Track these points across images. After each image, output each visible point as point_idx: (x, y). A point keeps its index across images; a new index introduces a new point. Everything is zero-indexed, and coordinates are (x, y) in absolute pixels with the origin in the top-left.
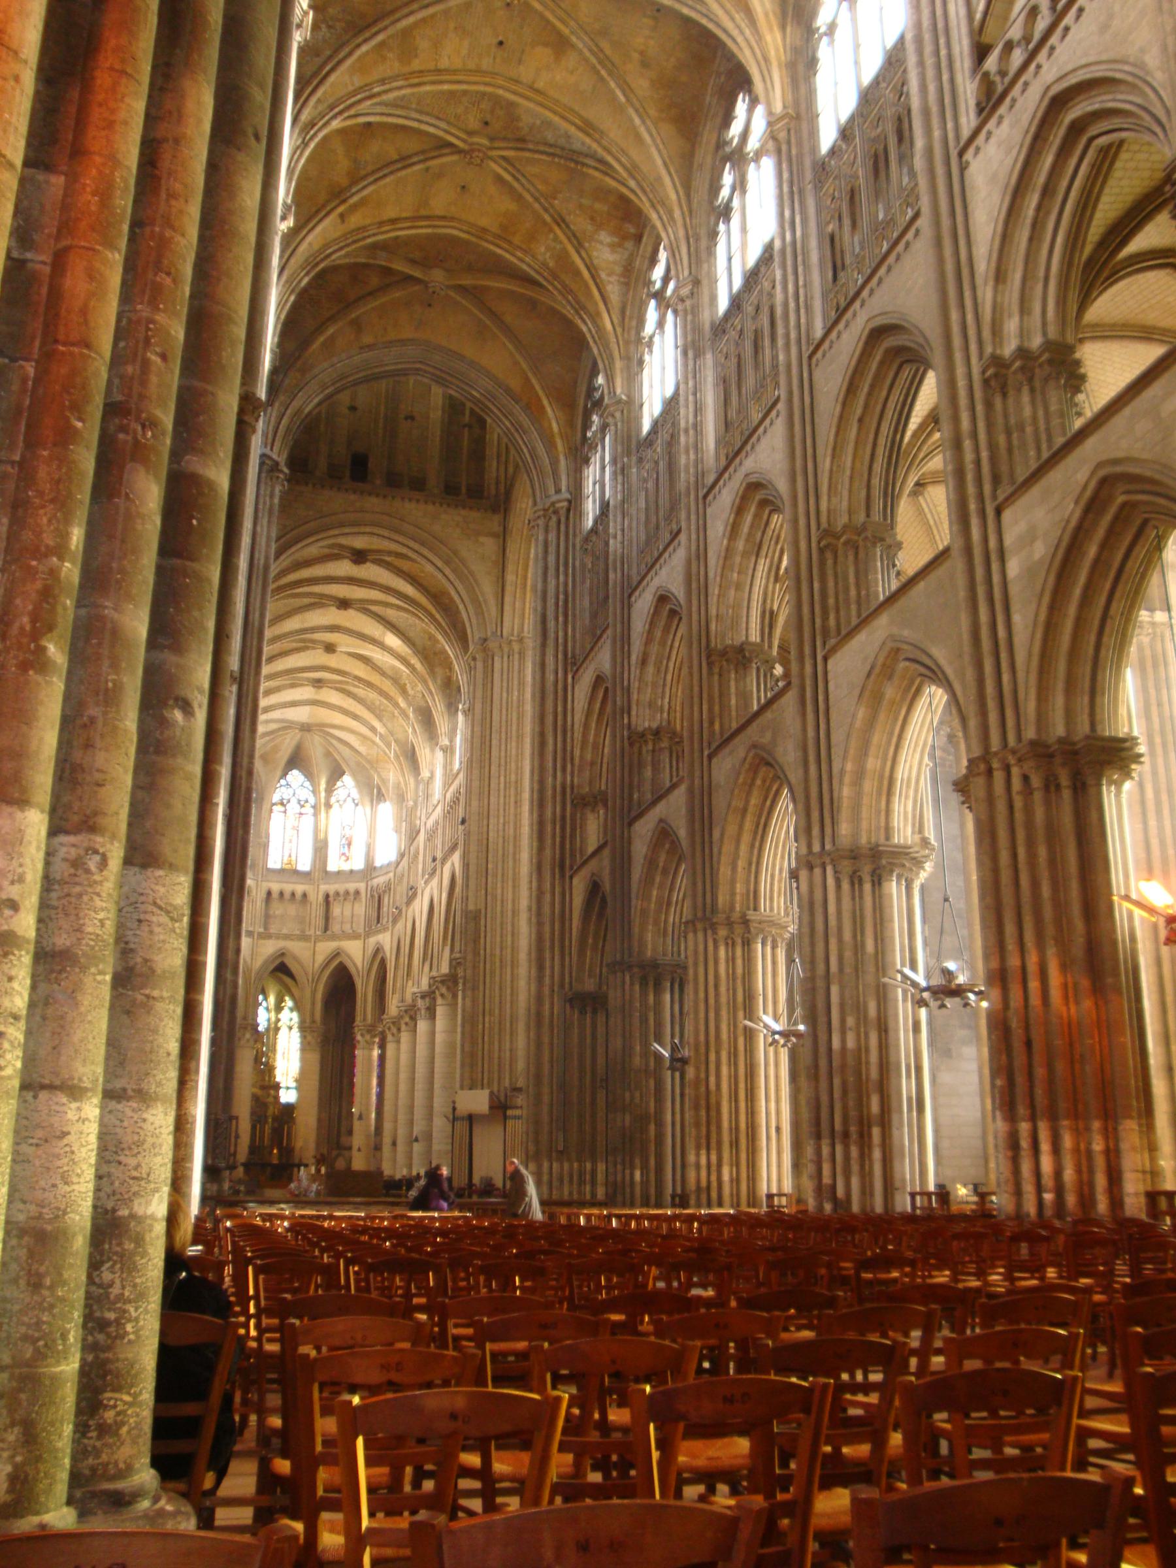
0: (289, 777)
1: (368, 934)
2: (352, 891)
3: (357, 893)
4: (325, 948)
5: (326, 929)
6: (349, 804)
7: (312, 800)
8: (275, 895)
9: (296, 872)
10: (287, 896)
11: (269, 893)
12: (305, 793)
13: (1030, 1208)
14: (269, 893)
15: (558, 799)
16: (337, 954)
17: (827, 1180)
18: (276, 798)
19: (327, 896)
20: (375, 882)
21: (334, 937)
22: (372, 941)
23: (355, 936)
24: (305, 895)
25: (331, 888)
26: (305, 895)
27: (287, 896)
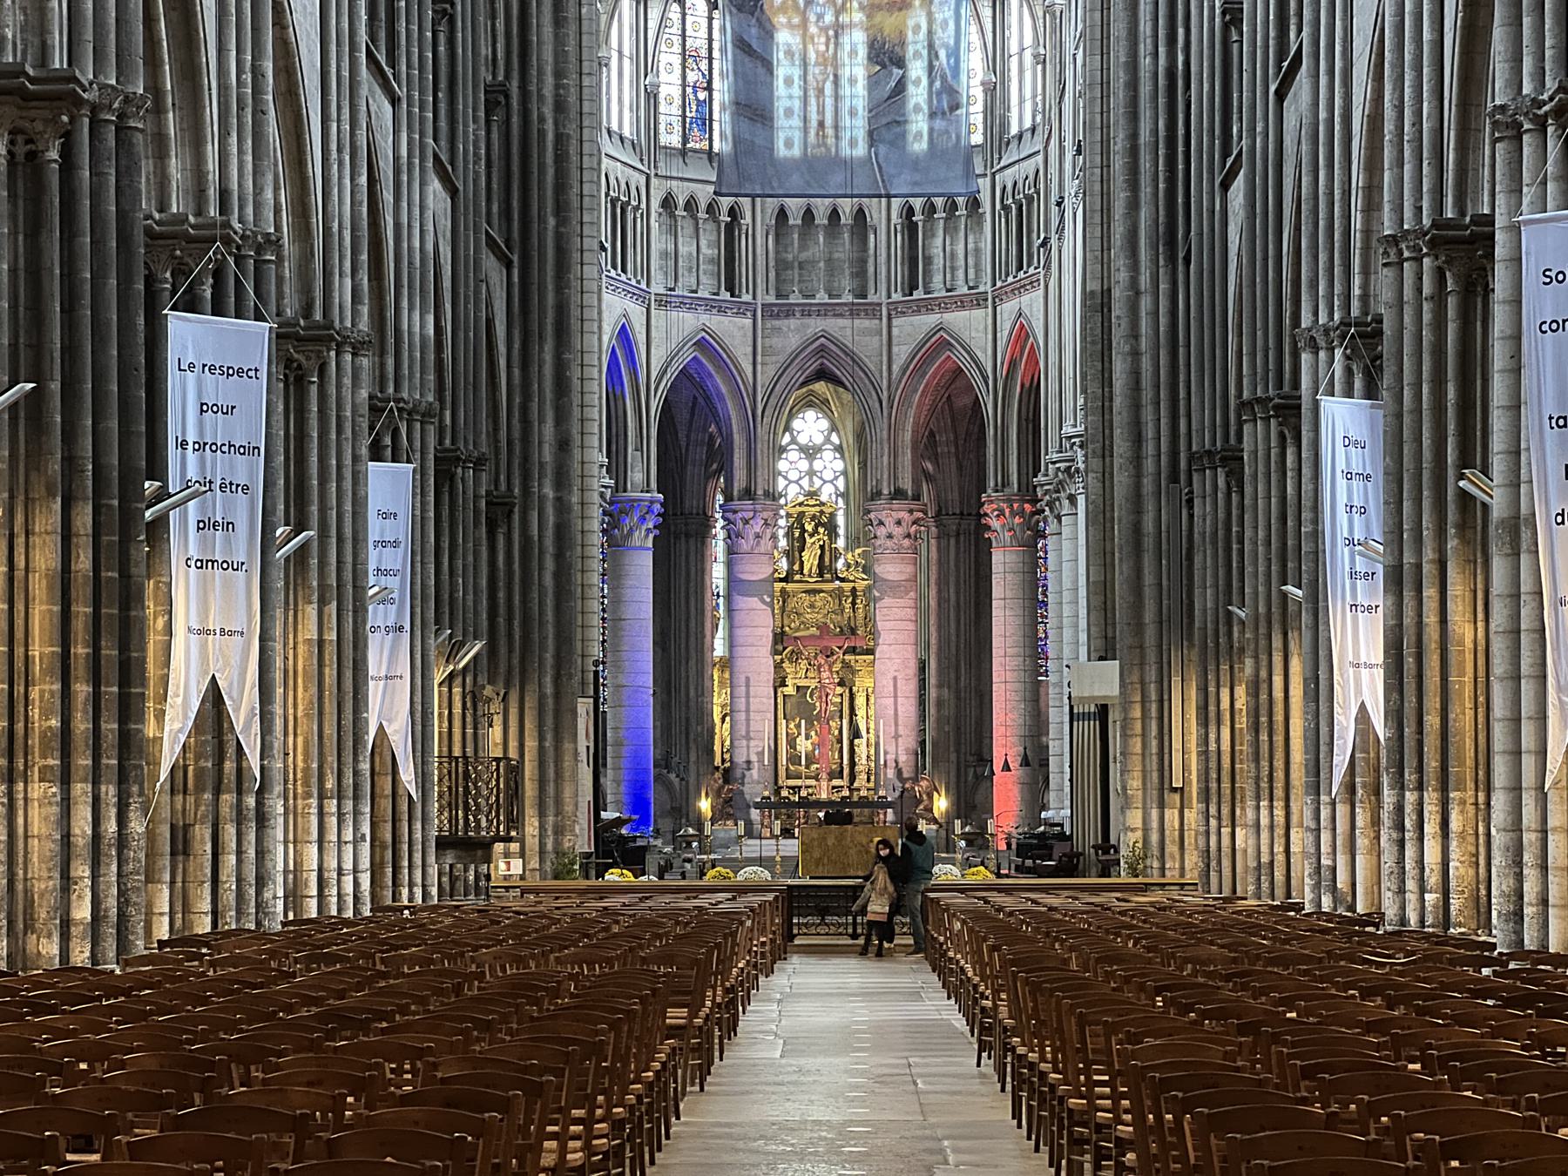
1: (998, 298)
4: (912, 329)
5: (913, 287)
11: (782, 214)
13: (1413, 917)
15: (1161, 100)
16: (939, 344)
17: (1325, 861)
20: (1007, 177)
21: (927, 306)
22: (1008, 309)
23: (979, 301)
24: (860, 214)
26: (860, 214)
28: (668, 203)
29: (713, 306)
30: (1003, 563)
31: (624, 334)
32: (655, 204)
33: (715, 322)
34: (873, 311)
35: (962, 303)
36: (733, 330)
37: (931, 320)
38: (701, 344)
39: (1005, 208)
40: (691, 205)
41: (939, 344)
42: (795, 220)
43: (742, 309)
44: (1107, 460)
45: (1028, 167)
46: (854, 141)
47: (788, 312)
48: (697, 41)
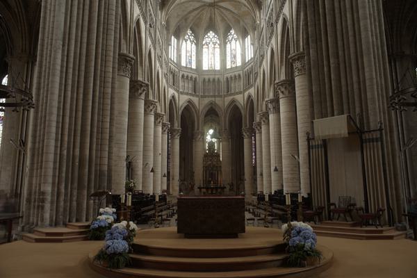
0: (209, 34)
2: (237, 75)
3: (239, 75)
4: (228, 99)
6: (233, 41)
7: (218, 42)
8: (207, 80)
9: (215, 71)
10: (211, 80)
11: (204, 80)
12: (215, 40)
14: (204, 80)
16: (233, 101)
18: (204, 42)
19: (227, 78)
22: (246, 94)
24: (218, 79)
25: (229, 75)
26: (218, 79)
27: (211, 80)
28: (183, 76)
29: (191, 94)
30: (246, 141)
31: (173, 97)
32: (181, 76)
33: (191, 98)
34: (221, 96)
35: (237, 93)
36: (195, 100)
37: (232, 97)
38: (189, 102)
39: (246, 75)
40: (187, 76)
41: (233, 101)
42: (207, 80)
43: (197, 96)
44: (318, 43)
45: (250, 65)
46: (218, 67)
47: (205, 97)
48: (189, 49)
